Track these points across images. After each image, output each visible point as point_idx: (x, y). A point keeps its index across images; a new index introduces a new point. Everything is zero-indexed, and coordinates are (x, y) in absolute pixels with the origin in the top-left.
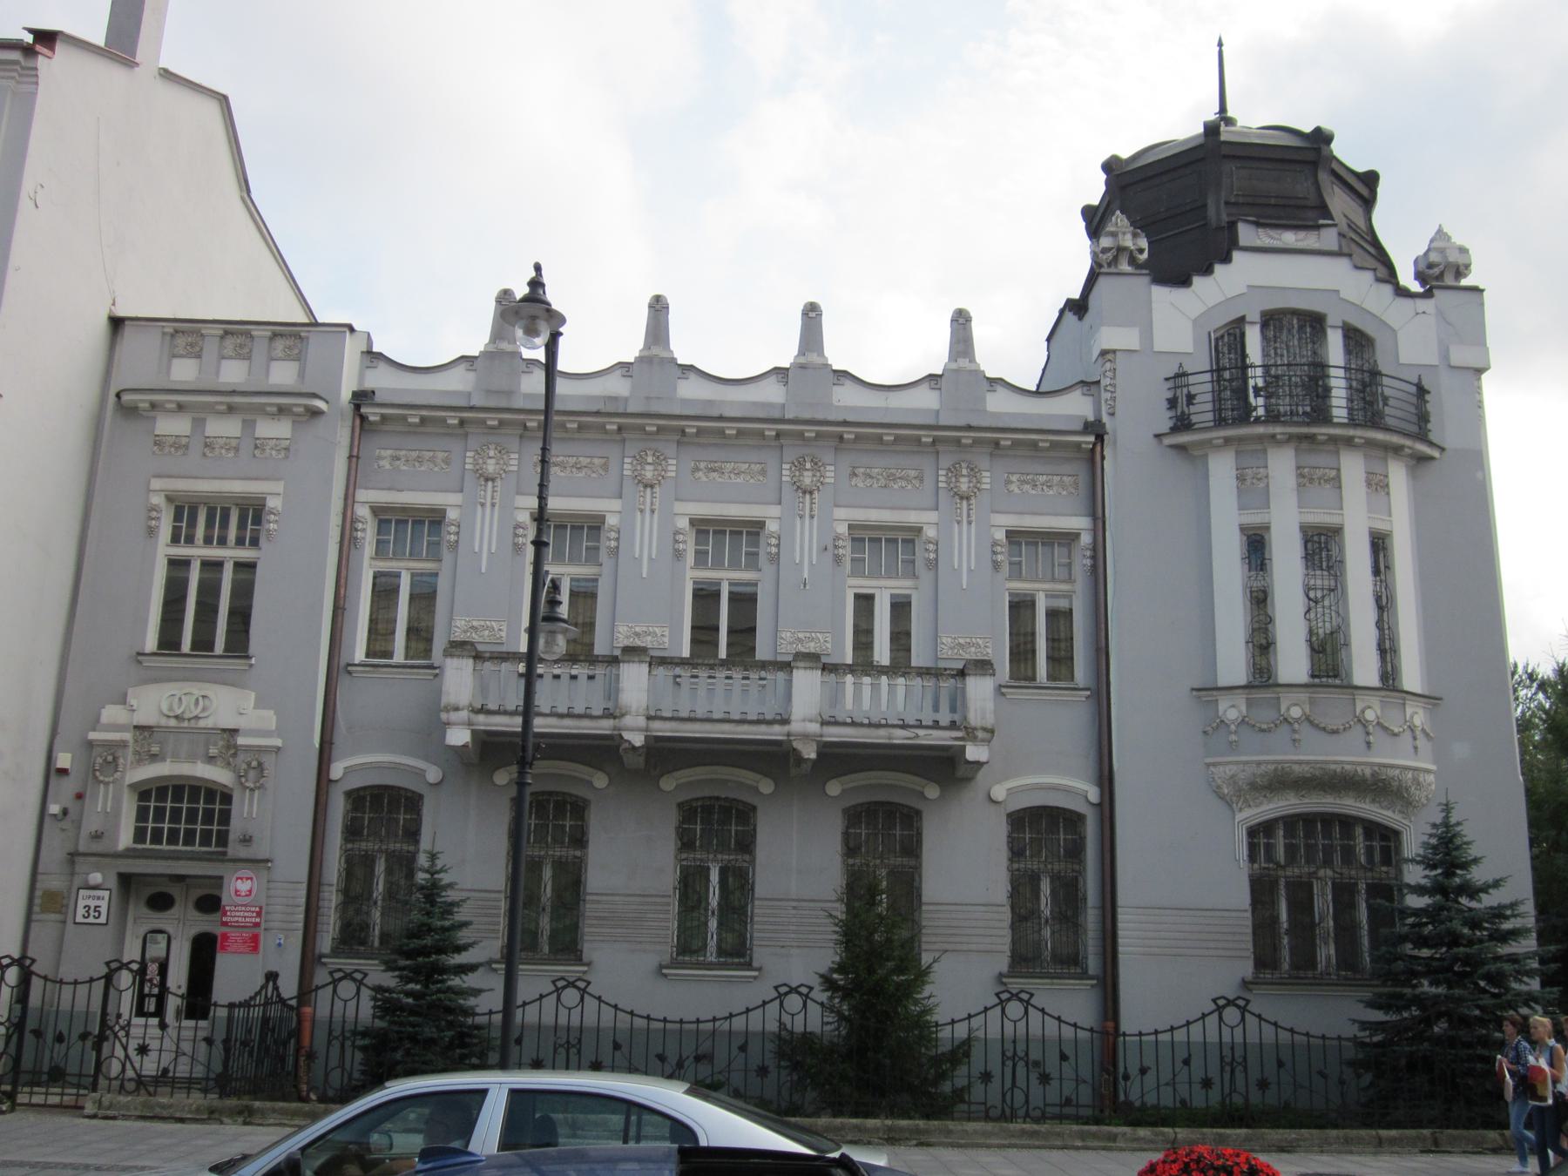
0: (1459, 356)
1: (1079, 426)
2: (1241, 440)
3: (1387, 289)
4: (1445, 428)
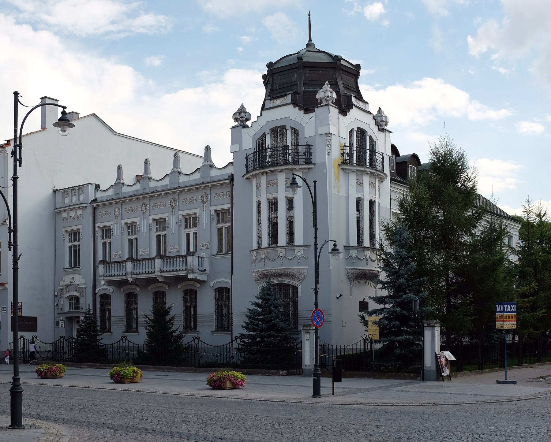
0: (322, 130)
4: (316, 158)
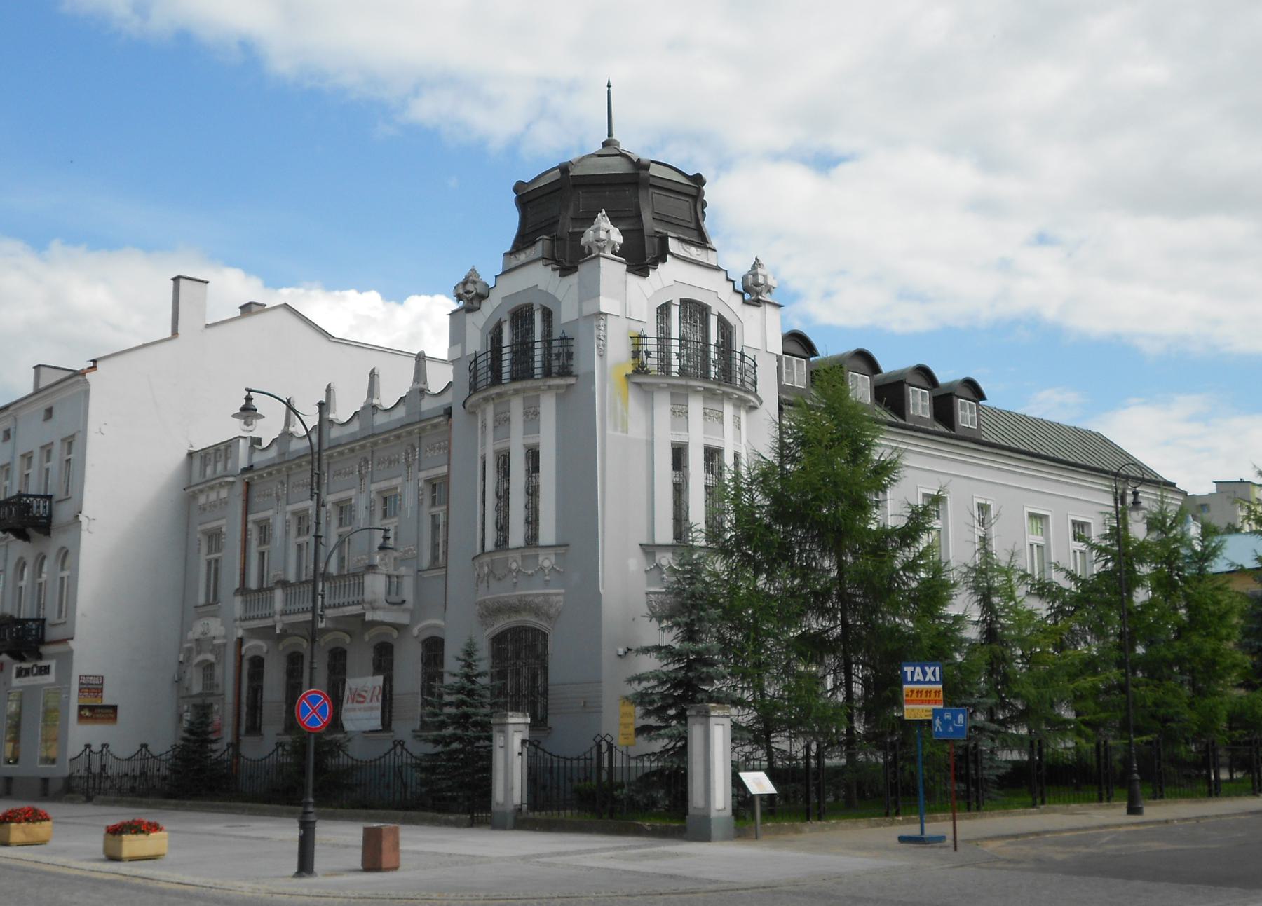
4: (579, 366)
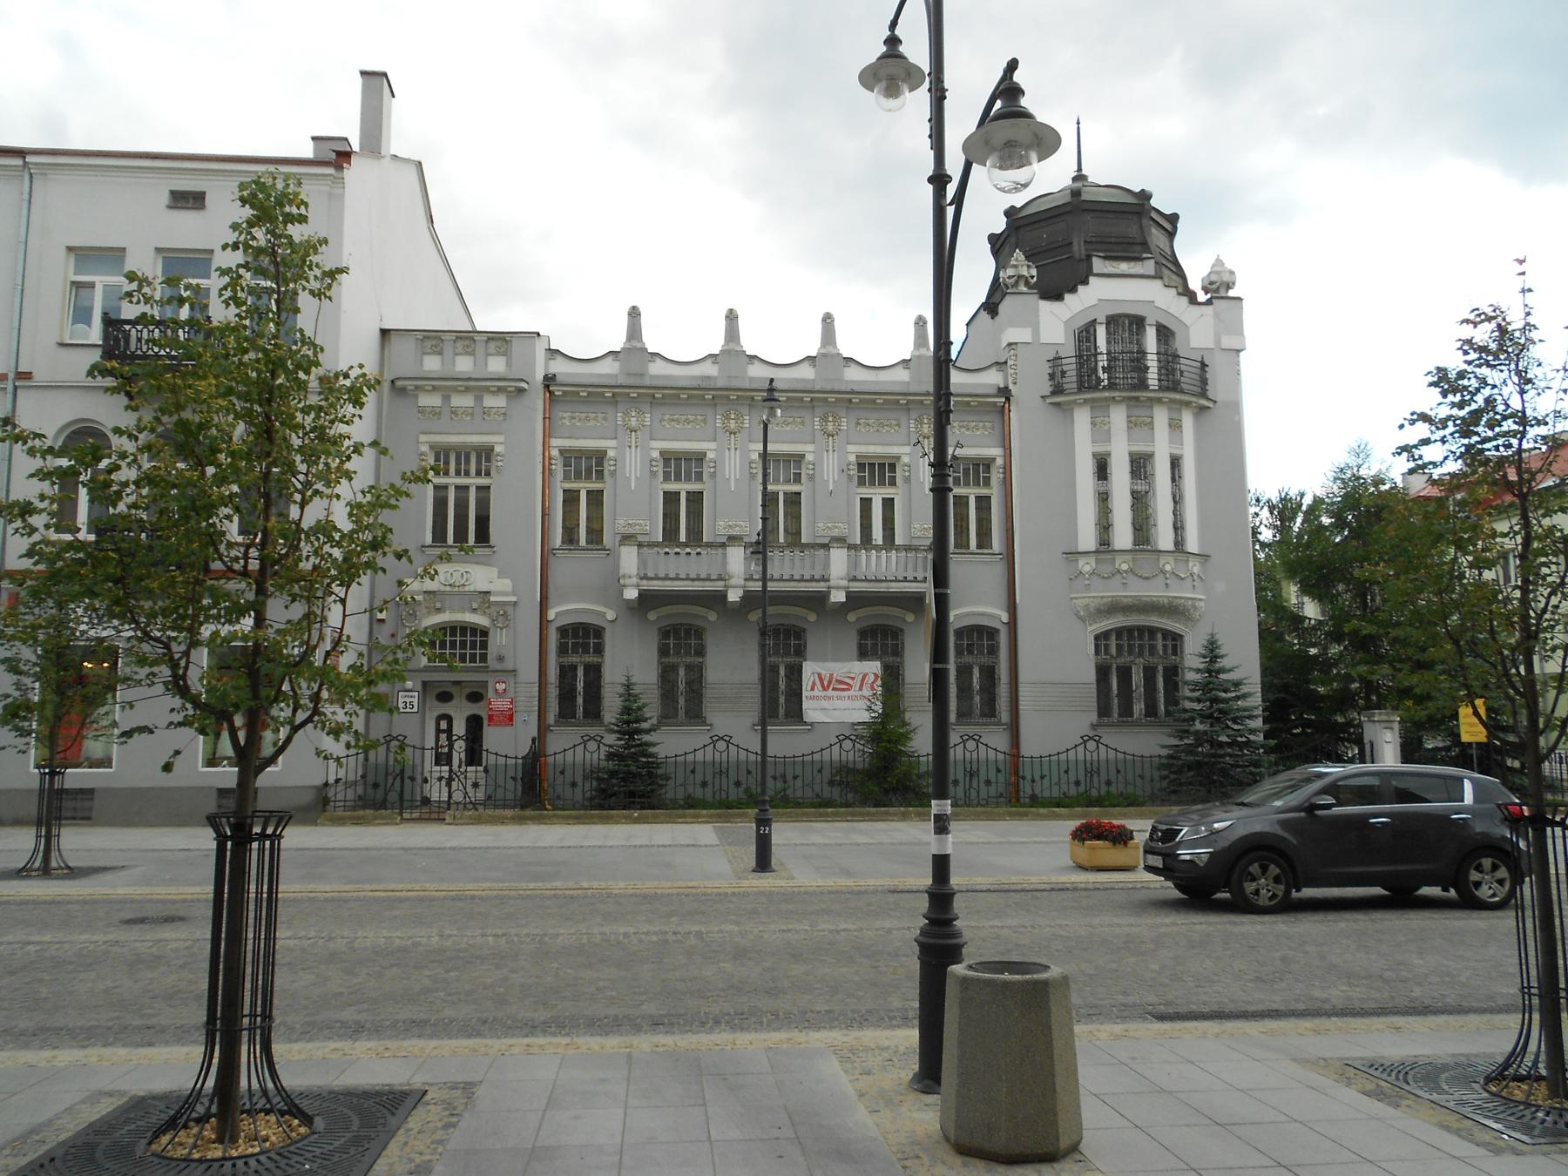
0: (1228, 342)
1: (994, 391)
2: (1093, 400)
3: (1185, 300)
4: (1217, 389)
